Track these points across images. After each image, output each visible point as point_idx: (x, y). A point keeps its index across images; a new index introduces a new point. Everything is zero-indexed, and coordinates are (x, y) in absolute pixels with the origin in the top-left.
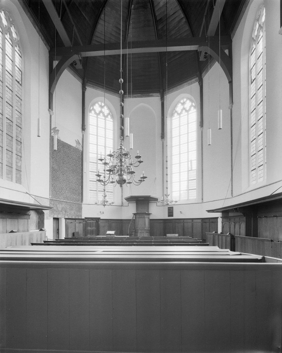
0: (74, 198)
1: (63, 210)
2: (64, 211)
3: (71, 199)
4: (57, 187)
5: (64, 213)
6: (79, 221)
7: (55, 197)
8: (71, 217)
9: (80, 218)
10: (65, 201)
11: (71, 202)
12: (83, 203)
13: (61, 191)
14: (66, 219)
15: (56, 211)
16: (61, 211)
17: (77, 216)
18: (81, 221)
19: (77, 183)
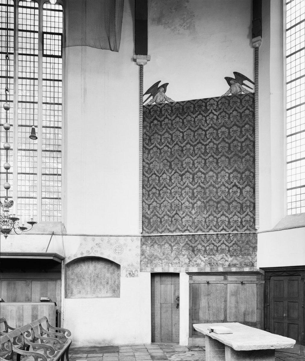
0: (223, 222)
1: (184, 255)
2: (186, 256)
3: (208, 227)
4: (163, 209)
5: (187, 261)
6: (238, 278)
7: (156, 230)
8: (211, 269)
9: (247, 269)
10: (187, 233)
11: (211, 232)
12: (258, 231)
13: (176, 213)
14: (190, 274)
15: (160, 259)
16: (176, 257)
17: (235, 265)
18: (254, 278)
19: (235, 181)
